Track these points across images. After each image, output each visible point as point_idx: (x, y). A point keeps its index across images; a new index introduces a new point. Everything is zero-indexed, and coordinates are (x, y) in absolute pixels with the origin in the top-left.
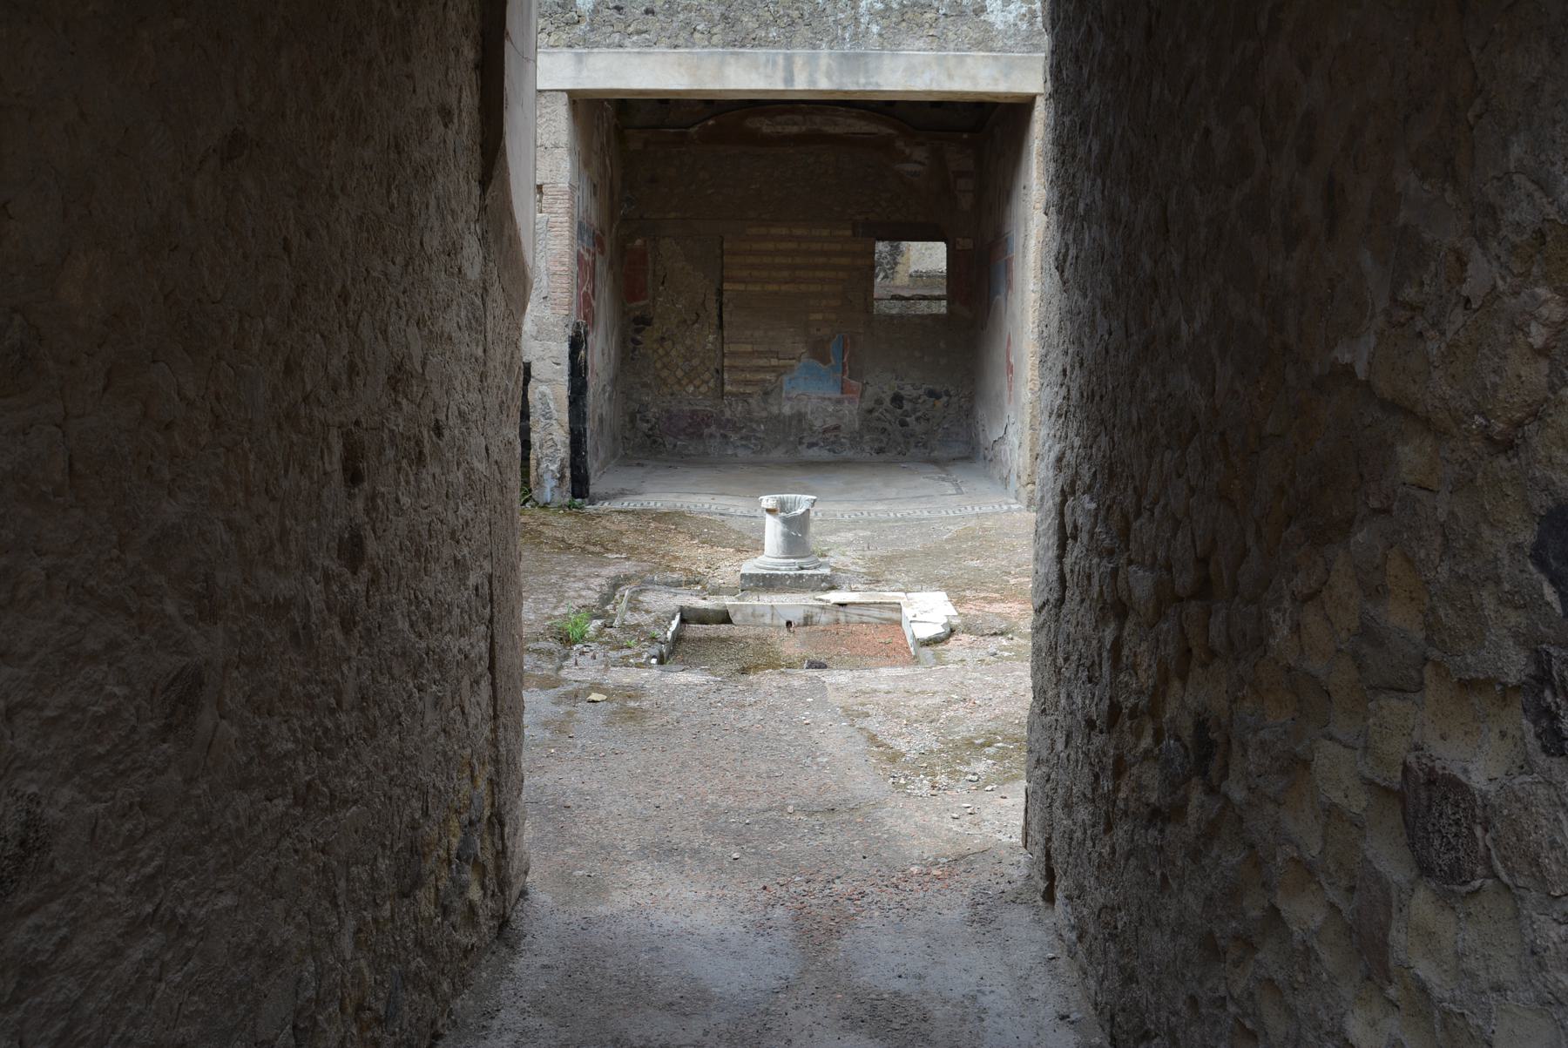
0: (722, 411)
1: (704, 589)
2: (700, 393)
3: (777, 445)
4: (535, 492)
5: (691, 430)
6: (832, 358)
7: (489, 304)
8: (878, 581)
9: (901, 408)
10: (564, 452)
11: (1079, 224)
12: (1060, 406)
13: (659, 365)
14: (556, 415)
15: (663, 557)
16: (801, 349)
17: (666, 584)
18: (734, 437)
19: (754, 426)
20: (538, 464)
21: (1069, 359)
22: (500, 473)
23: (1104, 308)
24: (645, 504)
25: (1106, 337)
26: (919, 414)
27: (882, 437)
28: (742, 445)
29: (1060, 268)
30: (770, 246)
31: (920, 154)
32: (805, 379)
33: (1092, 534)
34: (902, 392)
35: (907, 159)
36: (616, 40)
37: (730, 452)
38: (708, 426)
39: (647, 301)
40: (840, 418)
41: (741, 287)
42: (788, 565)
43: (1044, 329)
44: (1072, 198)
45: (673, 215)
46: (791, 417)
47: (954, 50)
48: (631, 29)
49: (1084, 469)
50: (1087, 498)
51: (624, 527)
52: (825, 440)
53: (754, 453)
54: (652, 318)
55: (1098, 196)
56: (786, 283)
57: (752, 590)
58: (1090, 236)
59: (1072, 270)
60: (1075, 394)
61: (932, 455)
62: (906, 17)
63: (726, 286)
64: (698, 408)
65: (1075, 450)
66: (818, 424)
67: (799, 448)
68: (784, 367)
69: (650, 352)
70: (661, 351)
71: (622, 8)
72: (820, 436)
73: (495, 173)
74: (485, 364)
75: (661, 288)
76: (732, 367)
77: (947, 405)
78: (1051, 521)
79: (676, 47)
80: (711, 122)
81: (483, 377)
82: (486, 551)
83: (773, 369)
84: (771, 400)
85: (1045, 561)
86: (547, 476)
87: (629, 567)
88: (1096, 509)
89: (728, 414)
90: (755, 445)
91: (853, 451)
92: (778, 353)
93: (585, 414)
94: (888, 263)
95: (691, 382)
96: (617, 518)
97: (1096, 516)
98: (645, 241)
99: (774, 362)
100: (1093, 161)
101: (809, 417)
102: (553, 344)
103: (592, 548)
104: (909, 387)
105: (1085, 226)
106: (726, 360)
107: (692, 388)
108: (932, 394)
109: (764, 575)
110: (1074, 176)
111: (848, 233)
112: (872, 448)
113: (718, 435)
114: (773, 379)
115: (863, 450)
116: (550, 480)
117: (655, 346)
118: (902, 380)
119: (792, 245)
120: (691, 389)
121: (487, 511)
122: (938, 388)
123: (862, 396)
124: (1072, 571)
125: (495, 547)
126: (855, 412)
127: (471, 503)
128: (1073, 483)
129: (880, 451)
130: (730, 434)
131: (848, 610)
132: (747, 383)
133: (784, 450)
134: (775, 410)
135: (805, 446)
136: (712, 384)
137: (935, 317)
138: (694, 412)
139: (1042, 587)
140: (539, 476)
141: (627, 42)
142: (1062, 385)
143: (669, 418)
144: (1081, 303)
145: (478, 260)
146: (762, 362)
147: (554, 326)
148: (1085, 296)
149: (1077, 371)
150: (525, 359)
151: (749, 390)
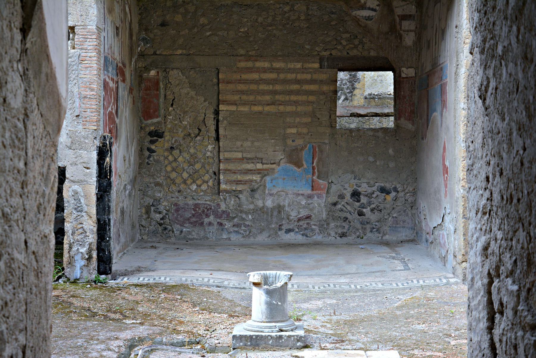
0: (218, 205)
1: (203, 348)
2: (203, 191)
3: (262, 231)
4: (67, 271)
5: (194, 219)
6: (304, 163)
7: (30, 127)
8: (343, 341)
9: (358, 201)
10: (92, 238)
11: (498, 62)
12: (484, 207)
13: (169, 169)
14: (86, 209)
15: (171, 322)
16: (280, 156)
17: (172, 344)
18: (228, 225)
19: (244, 216)
21: (491, 169)
22: (37, 261)
23: (519, 129)
24: (157, 278)
25: (521, 152)
26: (373, 206)
27: (344, 224)
28: (235, 231)
29: (483, 98)
30: (255, 76)
32: (284, 179)
33: (515, 312)
34: (360, 189)
37: (225, 236)
38: (207, 216)
39: (159, 119)
40: (311, 210)
41: (233, 108)
42: (270, 327)
43: (470, 144)
44: (492, 42)
45: (179, 52)
46: (273, 209)
49: (506, 257)
50: (509, 281)
51: (139, 298)
52: (299, 227)
54: (164, 132)
55: (514, 40)
56: (268, 105)
57: (241, 348)
58: (507, 72)
59: (492, 98)
60: (496, 197)
61: (384, 238)
63: (221, 107)
64: (199, 202)
65: (499, 242)
66: (293, 214)
67: (279, 233)
70: (171, 158)
72: (296, 223)
73: (34, 23)
74: (26, 174)
75: (171, 109)
77: (396, 199)
78: (481, 298)
81: (24, 185)
82: (22, 326)
83: (259, 172)
84: (257, 196)
85: (477, 331)
86: (78, 257)
87: (142, 331)
88: (518, 291)
89: (223, 207)
90: (245, 231)
92: (262, 159)
93: (109, 207)
94: (348, 88)
95: (194, 182)
96: (133, 290)
97: (518, 296)
98: (158, 72)
99: (259, 166)
100: (510, 11)
101: (287, 209)
103: (112, 316)
105: (503, 63)
106: (221, 165)
108: (383, 190)
109: (251, 337)
110: (494, 24)
111: (317, 65)
112: (336, 233)
113: (216, 223)
114: (259, 179)
115: (330, 235)
116: (80, 261)
119: (273, 76)
120: (194, 187)
121: (24, 293)
122: (388, 186)
123: (328, 192)
124: (501, 341)
125: (29, 322)
126: (323, 205)
127: (10, 287)
128: (497, 268)
129: (343, 235)
130: (225, 222)
132: (238, 182)
133: (267, 235)
134: (260, 204)
136: (210, 183)
137: (385, 130)
138: (196, 206)
139: (476, 353)
140: (71, 258)
142: (485, 189)
143: (177, 210)
144: (500, 125)
145: (21, 92)
146: (250, 166)
147: (85, 138)
148: (503, 120)
149: (498, 178)
150: (60, 164)
151: (239, 188)
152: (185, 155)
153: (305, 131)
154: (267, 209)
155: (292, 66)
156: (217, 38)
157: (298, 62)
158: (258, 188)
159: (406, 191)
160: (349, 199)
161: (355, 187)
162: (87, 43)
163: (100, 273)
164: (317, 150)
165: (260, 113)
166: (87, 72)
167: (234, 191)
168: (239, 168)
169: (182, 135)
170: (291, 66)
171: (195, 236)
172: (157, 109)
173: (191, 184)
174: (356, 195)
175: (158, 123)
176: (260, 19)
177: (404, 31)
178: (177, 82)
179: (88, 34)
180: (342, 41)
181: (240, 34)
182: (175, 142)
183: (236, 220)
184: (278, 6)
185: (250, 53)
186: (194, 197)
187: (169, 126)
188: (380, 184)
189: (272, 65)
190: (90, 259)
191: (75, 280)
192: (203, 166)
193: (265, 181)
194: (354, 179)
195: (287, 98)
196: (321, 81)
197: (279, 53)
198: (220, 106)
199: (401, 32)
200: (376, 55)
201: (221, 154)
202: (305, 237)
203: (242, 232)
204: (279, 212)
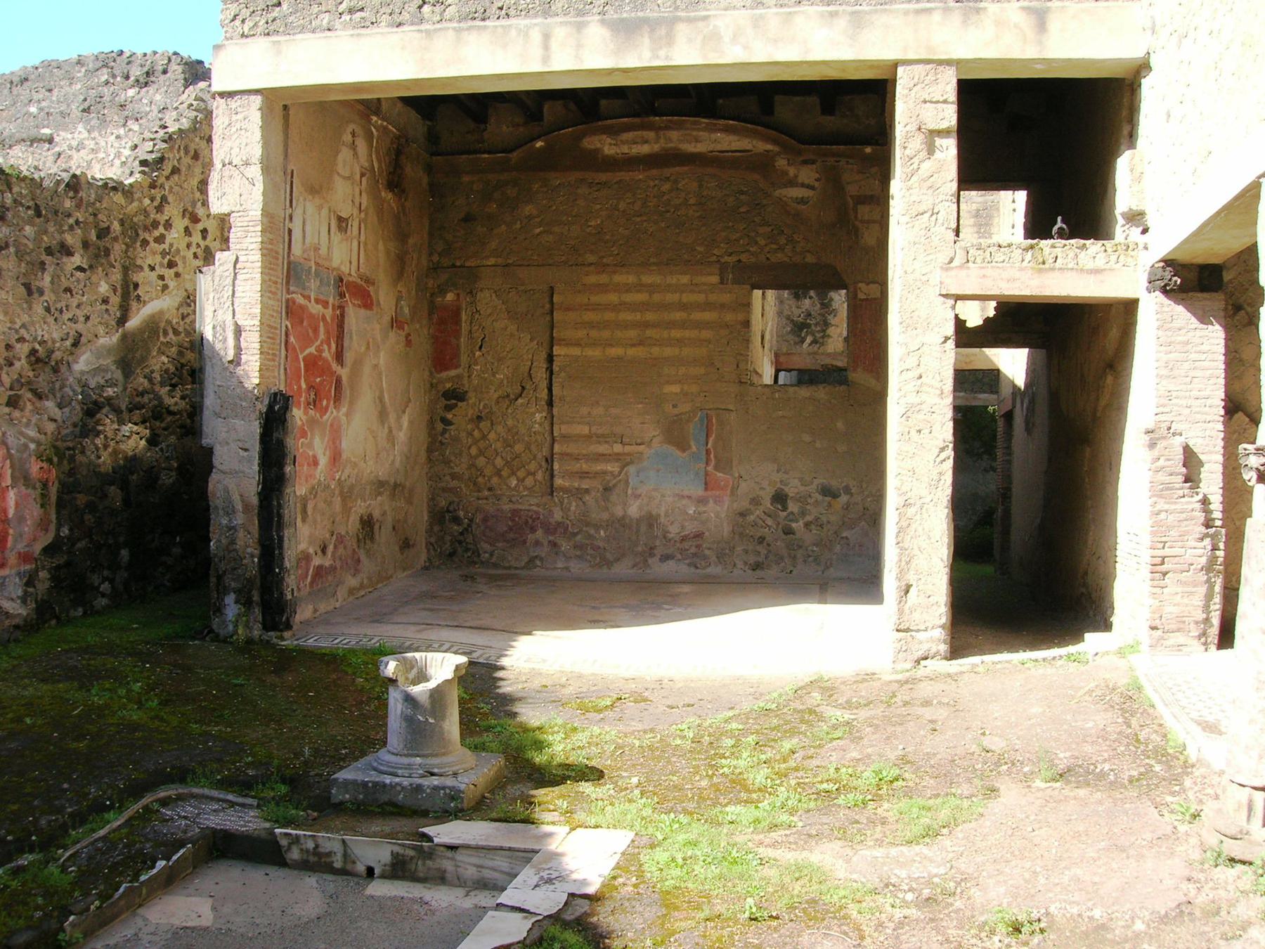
2: (526, 488)
5: (512, 535)
6: (692, 443)
9: (785, 508)
13: (474, 451)
16: (652, 432)
19: (592, 532)
26: (808, 518)
27: (759, 548)
30: (613, 298)
31: (807, 174)
34: (786, 489)
35: (792, 183)
36: (325, 22)
37: (560, 565)
38: (533, 530)
41: (576, 351)
45: (492, 261)
46: (639, 521)
48: (342, 8)
52: (682, 551)
56: (633, 345)
63: (557, 350)
64: (520, 507)
66: (674, 530)
69: (463, 434)
70: (476, 433)
75: (478, 353)
76: (563, 454)
77: (847, 507)
80: (539, 144)
83: (617, 457)
84: (613, 498)
89: (558, 516)
93: (280, 516)
94: (816, 325)
95: (514, 473)
99: (618, 448)
107: (515, 482)
108: (827, 491)
109: (365, 784)
111: (715, 279)
112: (746, 563)
113: (546, 543)
114: (616, 470)
117: (469, 427)
118: (786, 473)
119: (641, 297)
120: (514, 482)
122: (835, 484)
123: (732, 493)
129: (757, 567)
131: (460, 856)
132: (584, 475)
134: (619, 512)
135: (656, 559)
136: (539, 476)
138: (515, 512)
141: (337, 24)
150: (205, 442)
152: (500, 429)
153: (694, 389)
154: (631, 520)
155: (674, 281)
156: (551, 238)
157: (685, 273)
158: (615, 486)
159: (866, 493)
160: (769, 505)
161: (779, 485)
162: (249, 240)
164: (714, 421)
165: (620, 358)
168: (584, 452)
169: (496, 396)
170: (672, 280)
171: (513, 563)
172: (456, 355)
173: (509, 477)
174: (780, 498)
175: (459, 377)
176: (622, 206)
177: (862, 222)
178: (489, 311)
179: (251, 224)
180: (758, 239)
181: (588, 230)
182: (484, 407)
183: (579, 537)
184: (652, 184)
185: (605, 260)
186: (513, 499)
188: (821, 481)
189: (640, 280)
193: (626, 474)
194: (778, 472)
195: (665, 334)
196: (723, 306)
197: (652, 260)
199: (857, 223)
200: (814, 261)
201: (556, 428)
202: (693, 569)
204: (651, 526)
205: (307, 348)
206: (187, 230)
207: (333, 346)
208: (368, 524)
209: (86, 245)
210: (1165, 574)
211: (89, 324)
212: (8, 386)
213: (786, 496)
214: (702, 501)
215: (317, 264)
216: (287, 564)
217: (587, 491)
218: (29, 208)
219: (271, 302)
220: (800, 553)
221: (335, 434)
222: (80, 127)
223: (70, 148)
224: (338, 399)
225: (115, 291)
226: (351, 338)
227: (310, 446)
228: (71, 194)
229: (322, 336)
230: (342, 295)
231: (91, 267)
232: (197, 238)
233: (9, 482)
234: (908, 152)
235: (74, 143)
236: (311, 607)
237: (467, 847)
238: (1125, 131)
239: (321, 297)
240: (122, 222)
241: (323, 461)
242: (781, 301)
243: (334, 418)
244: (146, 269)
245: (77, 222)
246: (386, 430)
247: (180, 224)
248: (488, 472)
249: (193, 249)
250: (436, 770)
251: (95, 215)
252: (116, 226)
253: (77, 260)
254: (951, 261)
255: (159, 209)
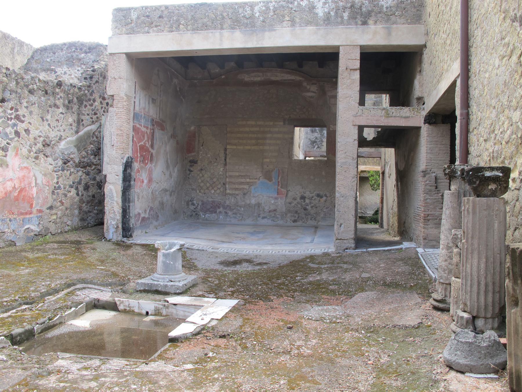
0: (225, 202)
5: (212, 209)
6: (273, 179)
10: (119, 217)
13: (200, 181)
14: (116, 199)
18: (230, 213)
19: (239, 208)
20: (107, 222)
26: (312, 205)
27: (295, 215)
30: (247, 129)
31: (314, 88)
34: (305, 195)
35: (309, 91)
36: (146, 30)
38: (219, 208)
39: (195, 153)
41: (234, 147)
46: (255, 205)
47: (299, 27)
53: (238, 220)
54: (197, 161)
56: (254, 145)
61: (318, 223)
62: (276, 12)
63: (228, 147)
66: (267, 208)
67: (259, 219)
68: (252, 182)
70: (201, 175)
71: (149, 16)
72: (268, 214)
75: (201, 148)
76: (230, 182)
77: (326, 201)
79: (172, 31)
80: (223, 77)
83: (248, 183)
86: (111, 227)
89: (228, 203)
90: (239, 217)
91: (282, 221)
92: (249, 176)
93: (129, 199)
94: (319, 141)
95: (213, 188)
98: (195, 128)
99: (248, 180)
101: (263, 205)
102: (115, 167)
104: (308, 192)
106: (227, 179)
108: (318, 196)
111: (282, 123)
112: (291, 220)
117: (199, 173)
118: (305, 189)
119: (257, 129)
120: (213, 191)
122: (321, 193)
123: (286, 196)
126: (283, 203)
129: (295, 221)
130: (228, 212)
131: (178, 307)
132: (236, 189)
134: (248, 202)
136: (222, 189)
138: (213, 202)
140: (108, 227)
141: (151, 31)
143: (203, 204)
146: (243, 180)
151: (237, 192)
163: (123, 237)
166: (119, 121)
167: (234, 194)
173: (211, 190)
174: (303, 198)
183: (234, 211)
187: (200, 157)
190: (118, 227)
191: (110, 240)
192: (218, 180)
194: (302, 189)
198: (227, 146)
202: (273, 222)
203: (238, 217)
205: (141, 142)
206: (101, 102)
207: (150, 143)
208: (162, 204)
209: (64, 105)
210: (429, 220)
211: (65, 132)
212: (34, 152)
213: (305, 197)
214: (276, 198)
215: (144, 114)
216: (131, 215)
217: (237, 195)
218: (43, 91)
219: (127, 126)
220: (309, 217)
221: (150, 172)
222: (65, 67)
223: (61, 74)
224: (151, 160)
225: (74, 122)
226: (156, 140)
227: (141, 176)
228: (59, 87)
229: (146, 139)
230: (153, 125)
231: (66, 113)
232: (105, 105)
233: (34, 185)
234: (342, 77)
235: (63, 72)
236: (140, 231)
237: (181, 304)
238: (419, 69)
239: (146, 125)
240: (77, 98)
241: (146, 181)
242: (307, 133)
243: (150, 167)
244: (86, 114)
245: (61, 97)
246: (169, 172)
247: (98, 100)
248: (205, 188)
249: (103, 109)
250: (173, 280)
251: (68, 95)
252: (75, 100)
253: (61, 110)
254: (357, 114)
255: (91, 94)
